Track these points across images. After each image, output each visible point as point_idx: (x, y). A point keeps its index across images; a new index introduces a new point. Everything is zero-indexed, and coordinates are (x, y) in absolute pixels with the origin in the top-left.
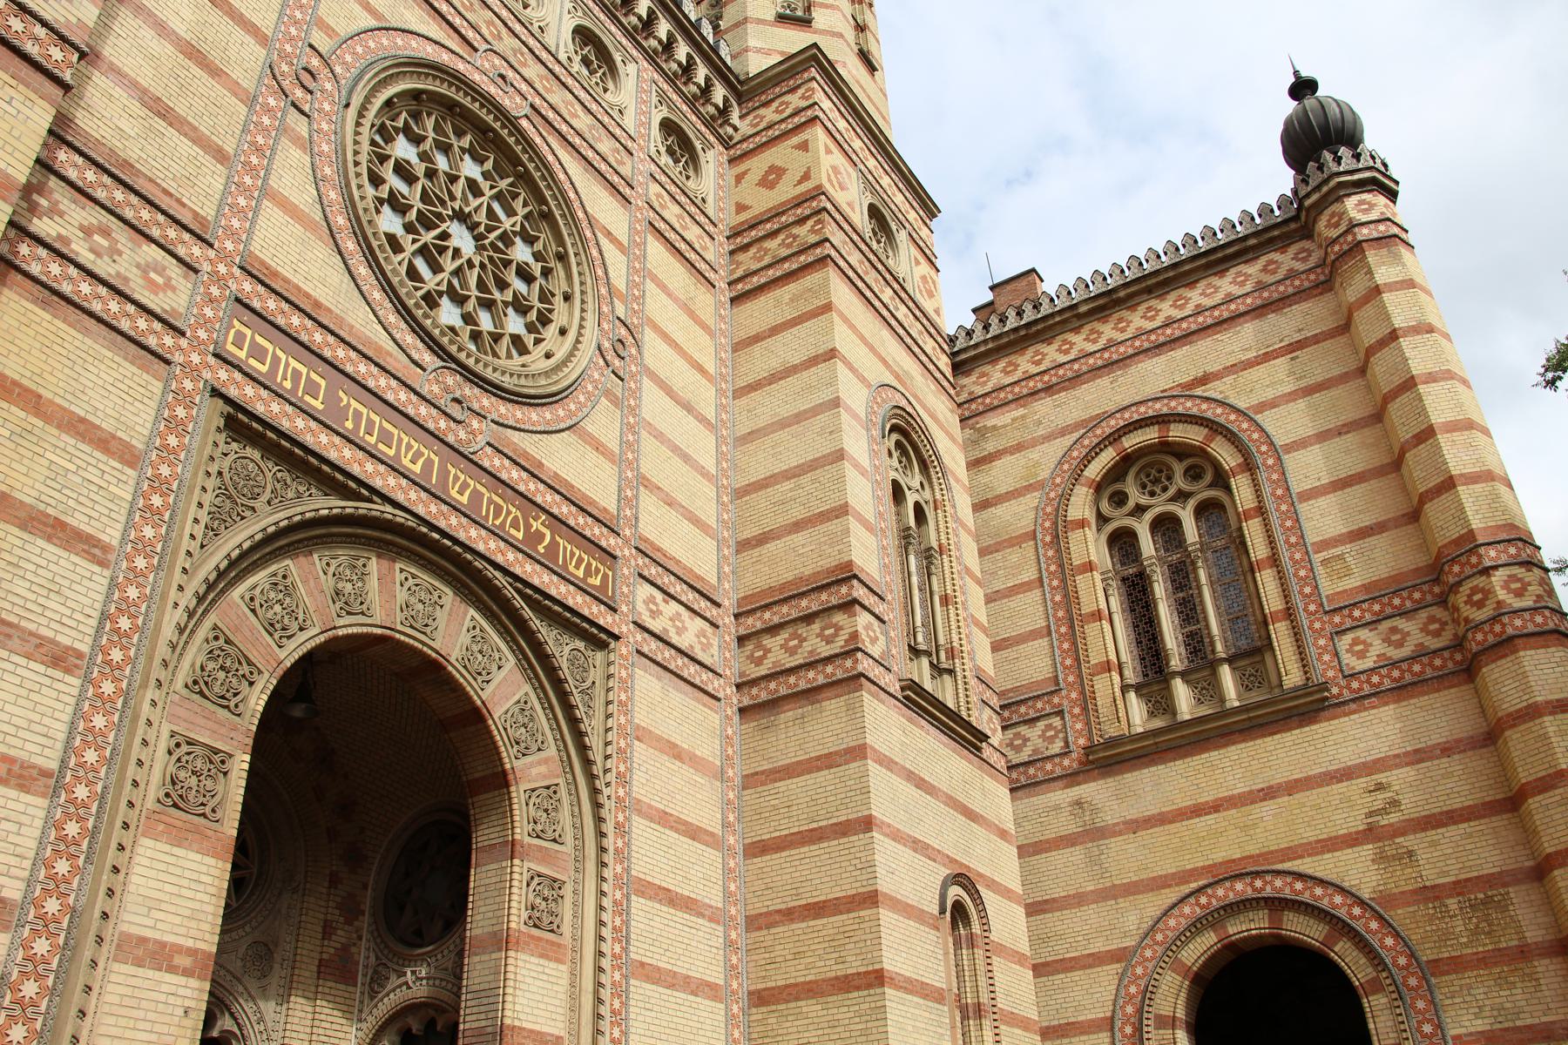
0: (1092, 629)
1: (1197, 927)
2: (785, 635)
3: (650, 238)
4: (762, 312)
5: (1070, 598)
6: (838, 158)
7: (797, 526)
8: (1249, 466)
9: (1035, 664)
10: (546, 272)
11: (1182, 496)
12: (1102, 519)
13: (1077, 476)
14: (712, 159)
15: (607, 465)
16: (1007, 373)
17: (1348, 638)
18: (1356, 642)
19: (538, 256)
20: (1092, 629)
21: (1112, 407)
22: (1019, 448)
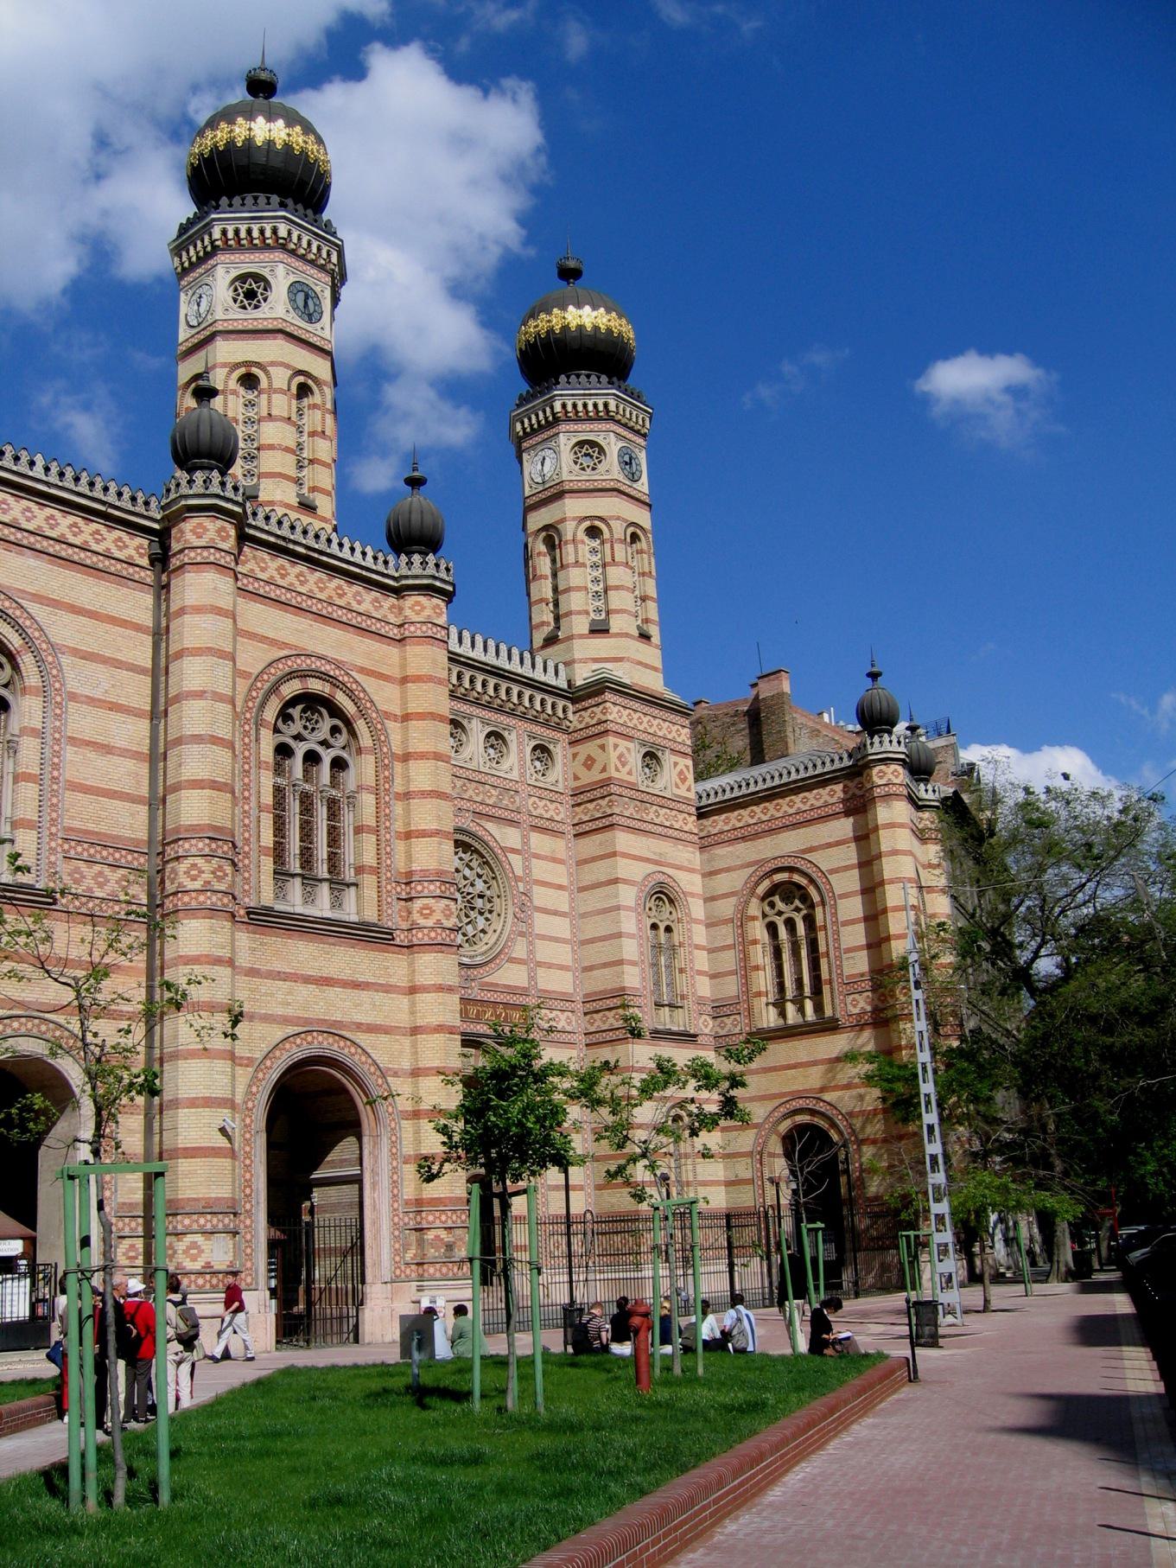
0: (754, 974)
1: (785, 1116)
2: (601, 1014)
3: (532, 834)
4: (591, 845)
5: (746, 958)
6: (623, 744)
7: (605, 965)
8: (823, 903)
9: (731, 987)
10: (489, 888)
11: (797, 910)
12: (765, 915)
13: (752, 892)
14: (559, 751)
15: (524, 968)
16: (726, 824)
17: (851, 997)
18: (854, 1000)
19: (485, 882)
20: (754, 974)
21: (770, 855)
22: (728, 870)
